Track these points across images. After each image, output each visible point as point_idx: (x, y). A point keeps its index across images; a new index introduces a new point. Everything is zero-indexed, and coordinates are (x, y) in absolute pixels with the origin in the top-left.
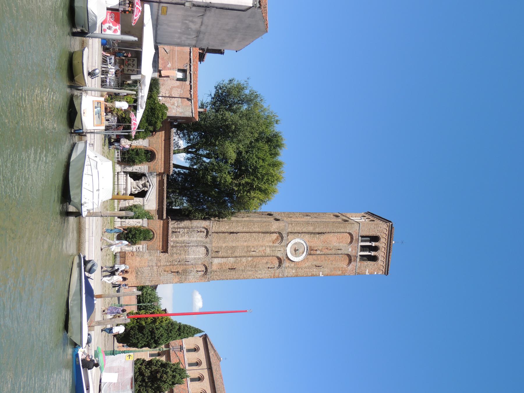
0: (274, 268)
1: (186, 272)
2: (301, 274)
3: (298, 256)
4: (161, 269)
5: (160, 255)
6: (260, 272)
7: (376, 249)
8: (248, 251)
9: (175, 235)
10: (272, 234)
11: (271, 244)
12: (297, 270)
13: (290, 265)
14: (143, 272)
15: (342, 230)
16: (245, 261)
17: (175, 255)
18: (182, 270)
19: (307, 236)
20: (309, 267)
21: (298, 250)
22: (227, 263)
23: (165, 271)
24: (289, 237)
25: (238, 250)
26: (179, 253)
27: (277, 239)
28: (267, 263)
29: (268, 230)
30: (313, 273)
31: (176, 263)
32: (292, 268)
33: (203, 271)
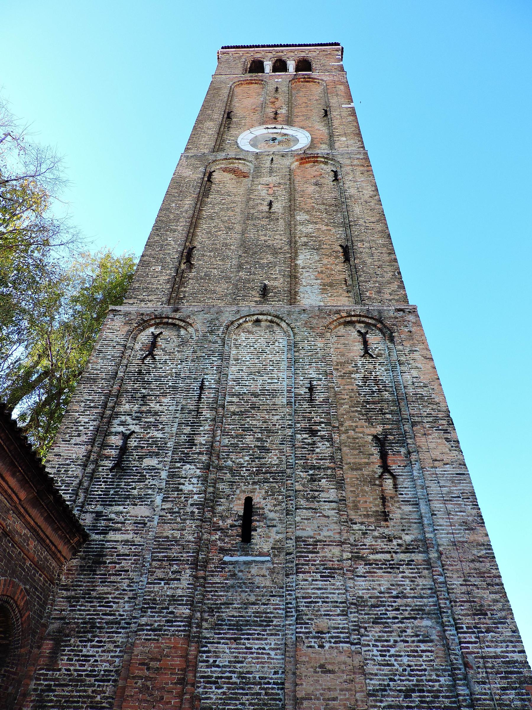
1: (374, 403)
4: (368, 541)
5: (266, 548)
8: (267, 218)
9: (141, 458)
14: (408, 693)
16: (309, 227)
17: (272, 459)
18: (369, 420)
20: (329, 125)
22: (319, 270)
23: (385, 516)
25: (263, 238)
26: (258, 440)
31: (323, 448)
33: (363, 335)
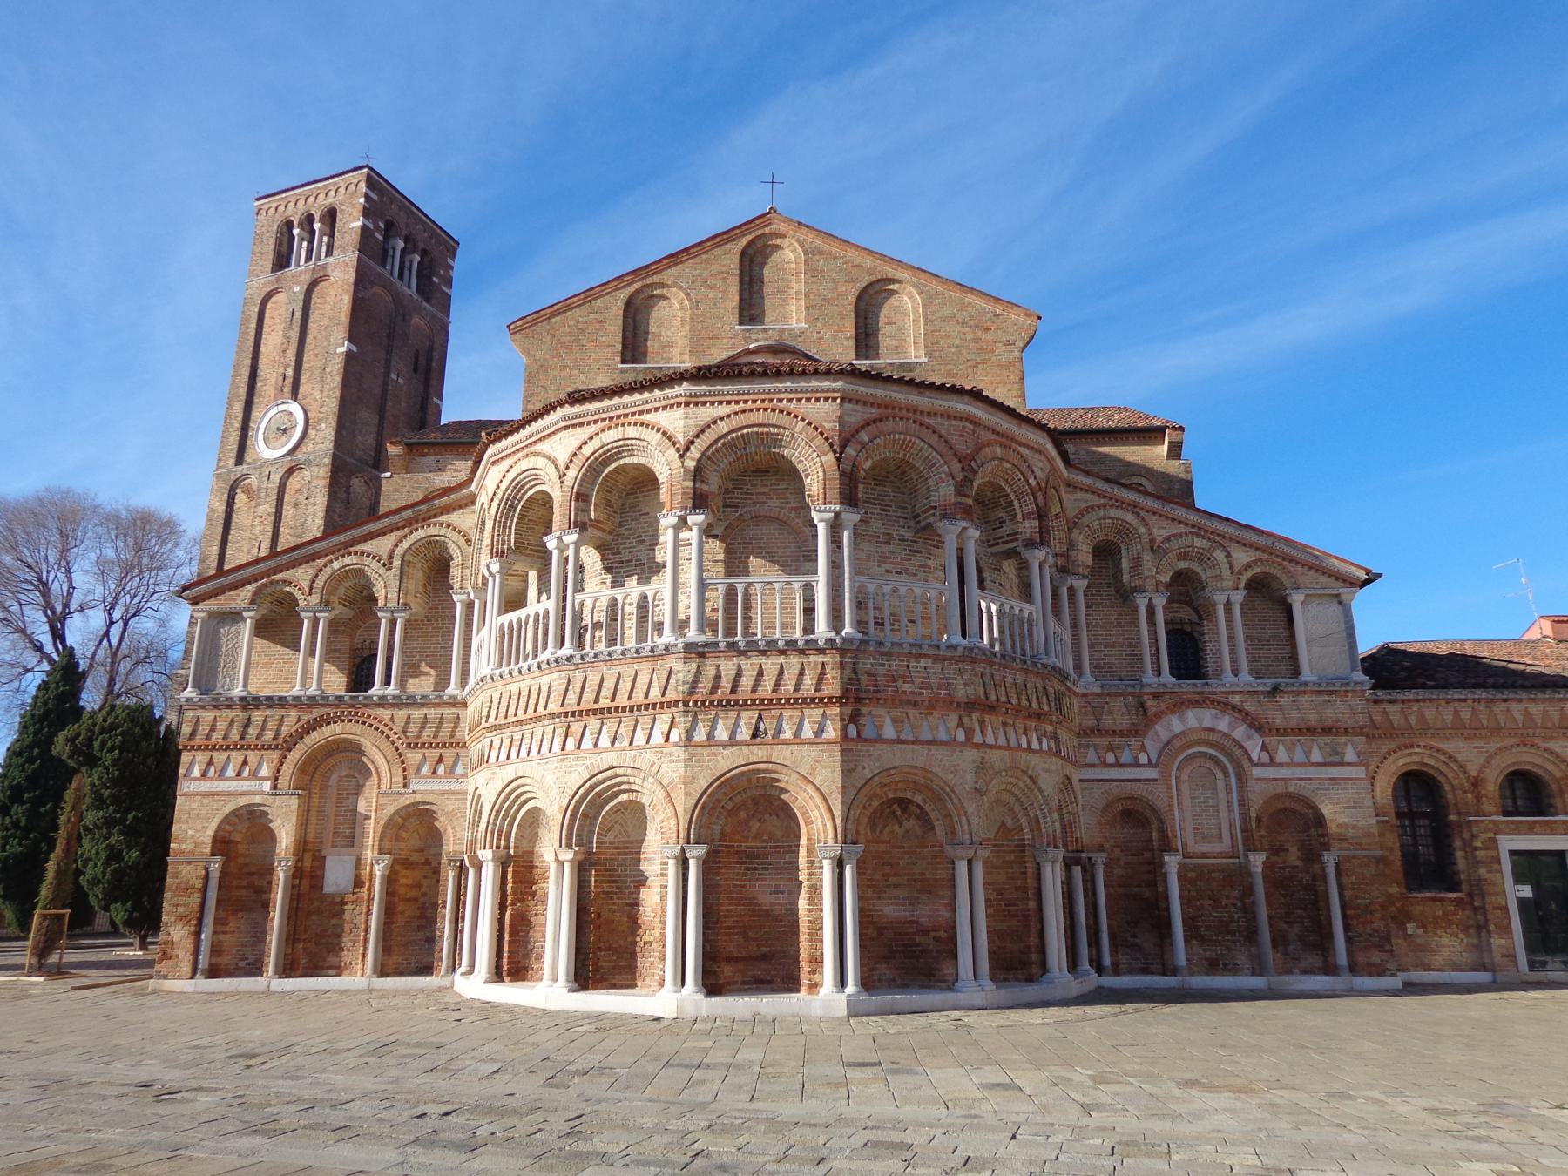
6: (309, 520)
7: (310, 219)
10: (236, 507)
11: (253, 503)
15: (253, 325)
19: (256, 413)
27: (247, 491)
28: (296, 505)
30: (335, 373)
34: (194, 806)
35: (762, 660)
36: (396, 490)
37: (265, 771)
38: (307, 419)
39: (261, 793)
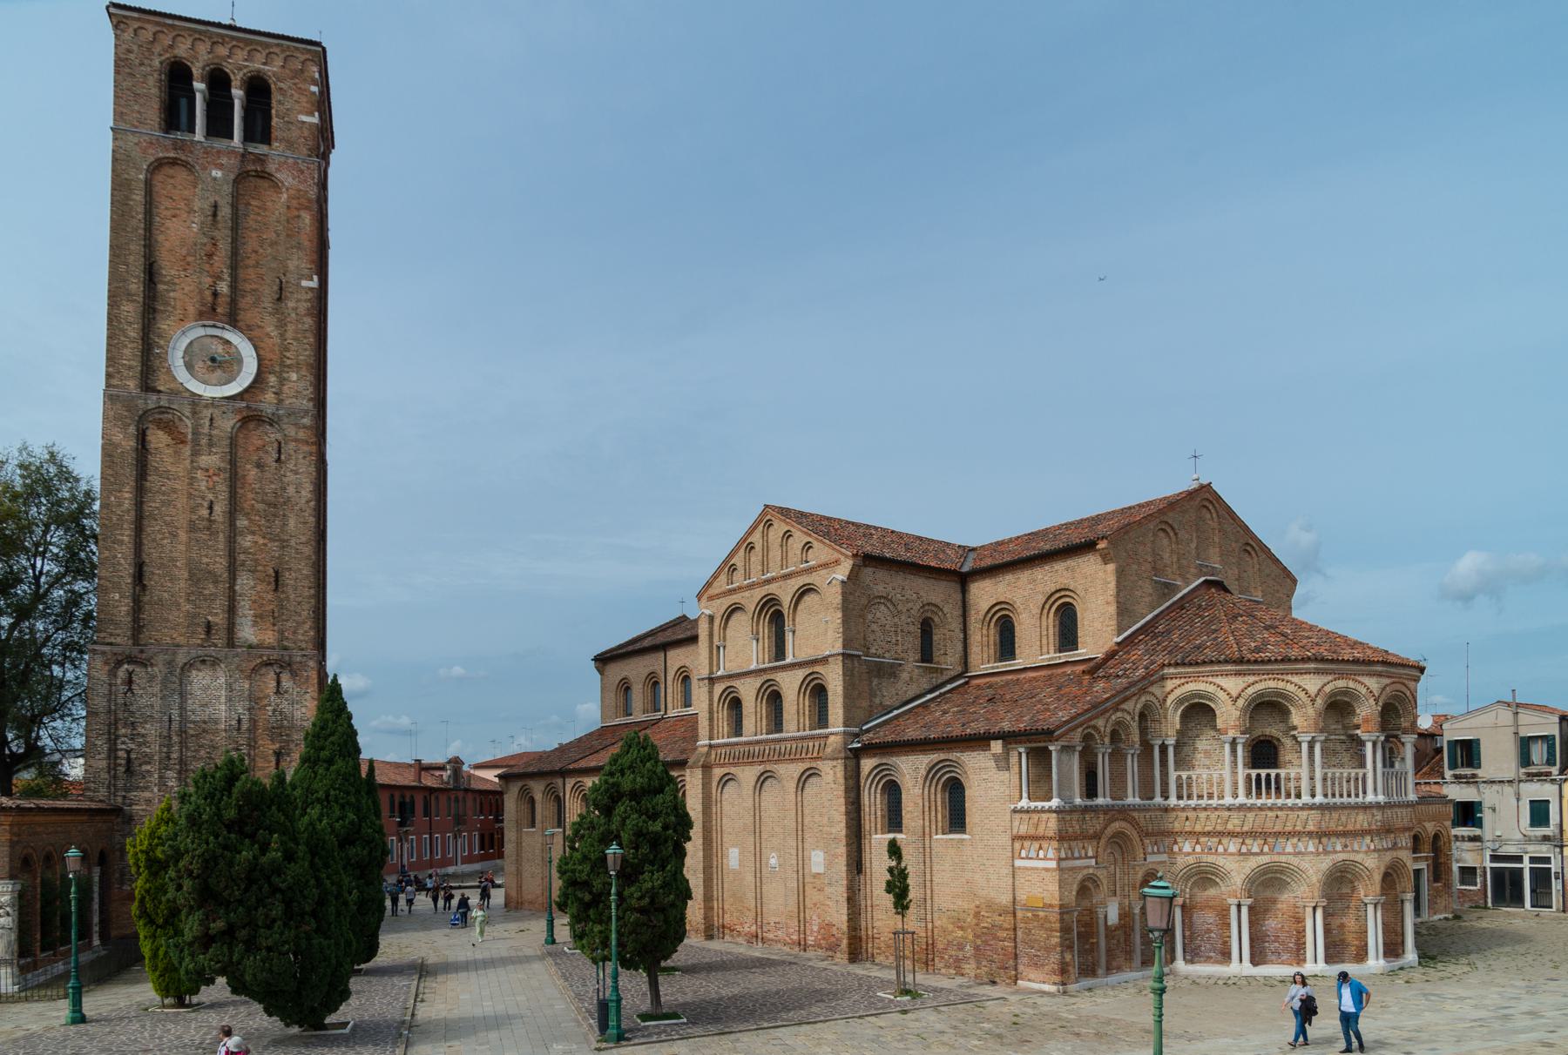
0: (280, 443)
2: (307, 353)
3: (240, 361)
11: (187, 450)
12: (289, 366)
13: (272, 387)
21: (213, 360)
24: (162, 388)
27: (169, 427)
29: (131, 459)
30: (302, 310)
32: (282, 381)
34: (1066, 876)
35: (1396, 810)
36: (851, 593)
37: (1090, 853)
38: (260, 359)
39: (1092, 867)
